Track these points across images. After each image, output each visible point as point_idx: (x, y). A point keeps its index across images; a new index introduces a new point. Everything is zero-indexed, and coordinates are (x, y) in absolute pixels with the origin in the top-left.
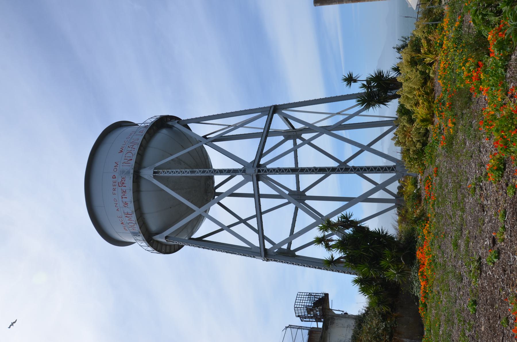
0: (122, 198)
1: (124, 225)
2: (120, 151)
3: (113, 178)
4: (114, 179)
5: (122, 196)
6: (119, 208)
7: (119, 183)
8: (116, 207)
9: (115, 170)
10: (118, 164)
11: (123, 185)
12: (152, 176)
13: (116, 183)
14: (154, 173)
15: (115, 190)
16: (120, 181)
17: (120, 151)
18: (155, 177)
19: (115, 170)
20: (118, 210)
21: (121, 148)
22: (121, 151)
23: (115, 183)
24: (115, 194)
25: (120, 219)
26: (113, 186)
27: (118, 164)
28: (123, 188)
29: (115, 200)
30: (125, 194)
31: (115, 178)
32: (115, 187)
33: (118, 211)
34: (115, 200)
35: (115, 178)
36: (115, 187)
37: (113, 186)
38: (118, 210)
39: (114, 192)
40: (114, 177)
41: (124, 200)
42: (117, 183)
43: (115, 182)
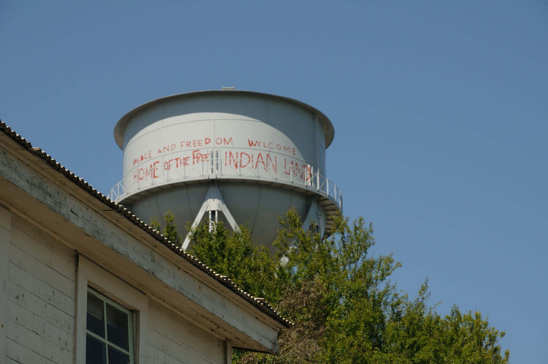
0: (177, 159)
1: (140, 161)
2: (252, 142)
3: (206, 139)
4: (203, 142)
5: (179, 158)
6: (163, 154)
7: (199, 151)
8: (164, 148)
9: (219, 141)
10: (228, 144)
11: (196, 159)
12: (207, 210)
13: (199, 146)
14: (213, 212)
15: (188, 145)
16: (203, 152)
17: (252, 142)
18: (206, 214)
19: (219, 141)
20: (160, 151)
21: (257, 142)
22: (252, 143)
23: (199, 143)
24: (182, 146)
25: (147, 156)
26: (194, 141)
27: (228, 144)
28: (191, 159)
29: (173, 146)
30: (182, 164)
31: (206, 143)
32: (192, 144)
33: (159, 152)
34: (173, 146)
35: (206, 143)
36: (192, 144)
37: (194, 141)
38: (160, 151)
39: (185, 144)
40: (208, 141)
41: (174, 163)
42: (198, 148)
43: (200, 144)
